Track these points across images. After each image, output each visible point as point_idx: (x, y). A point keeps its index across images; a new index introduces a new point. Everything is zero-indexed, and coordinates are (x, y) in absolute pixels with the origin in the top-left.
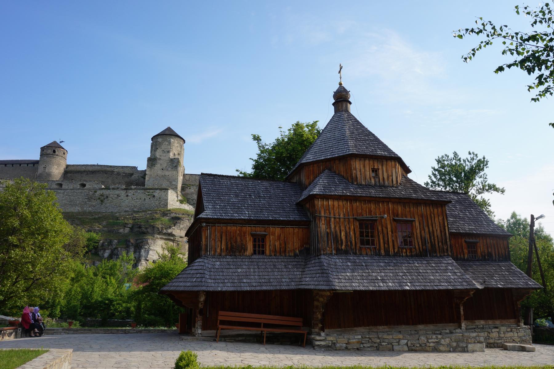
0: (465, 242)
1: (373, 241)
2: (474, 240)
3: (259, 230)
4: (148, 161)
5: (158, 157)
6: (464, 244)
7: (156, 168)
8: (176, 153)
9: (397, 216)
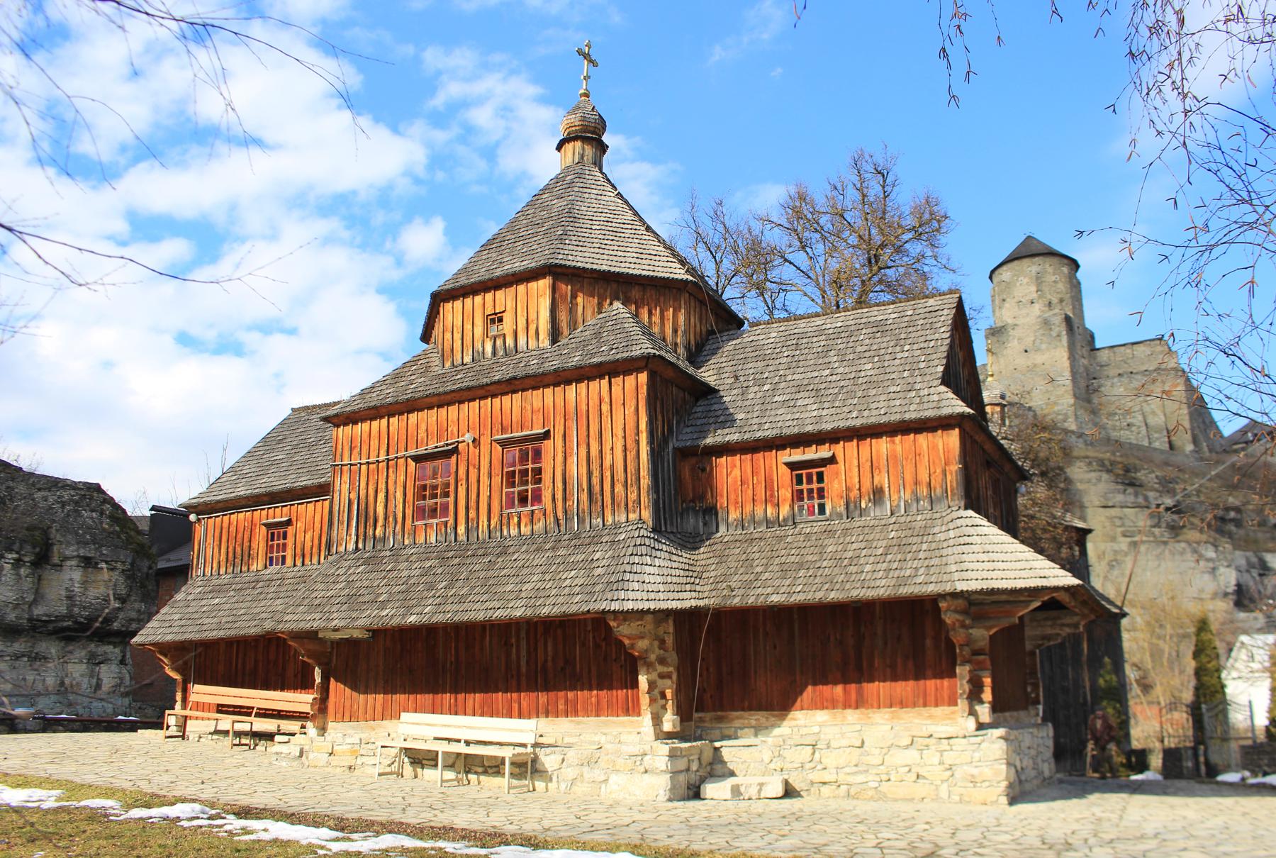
1: (445, 507)
3: (278, 514)
4: (987, 338)
5: (1010, 321)
7: (1008, 352)
8: (1055, 301)
9: (503, 430)
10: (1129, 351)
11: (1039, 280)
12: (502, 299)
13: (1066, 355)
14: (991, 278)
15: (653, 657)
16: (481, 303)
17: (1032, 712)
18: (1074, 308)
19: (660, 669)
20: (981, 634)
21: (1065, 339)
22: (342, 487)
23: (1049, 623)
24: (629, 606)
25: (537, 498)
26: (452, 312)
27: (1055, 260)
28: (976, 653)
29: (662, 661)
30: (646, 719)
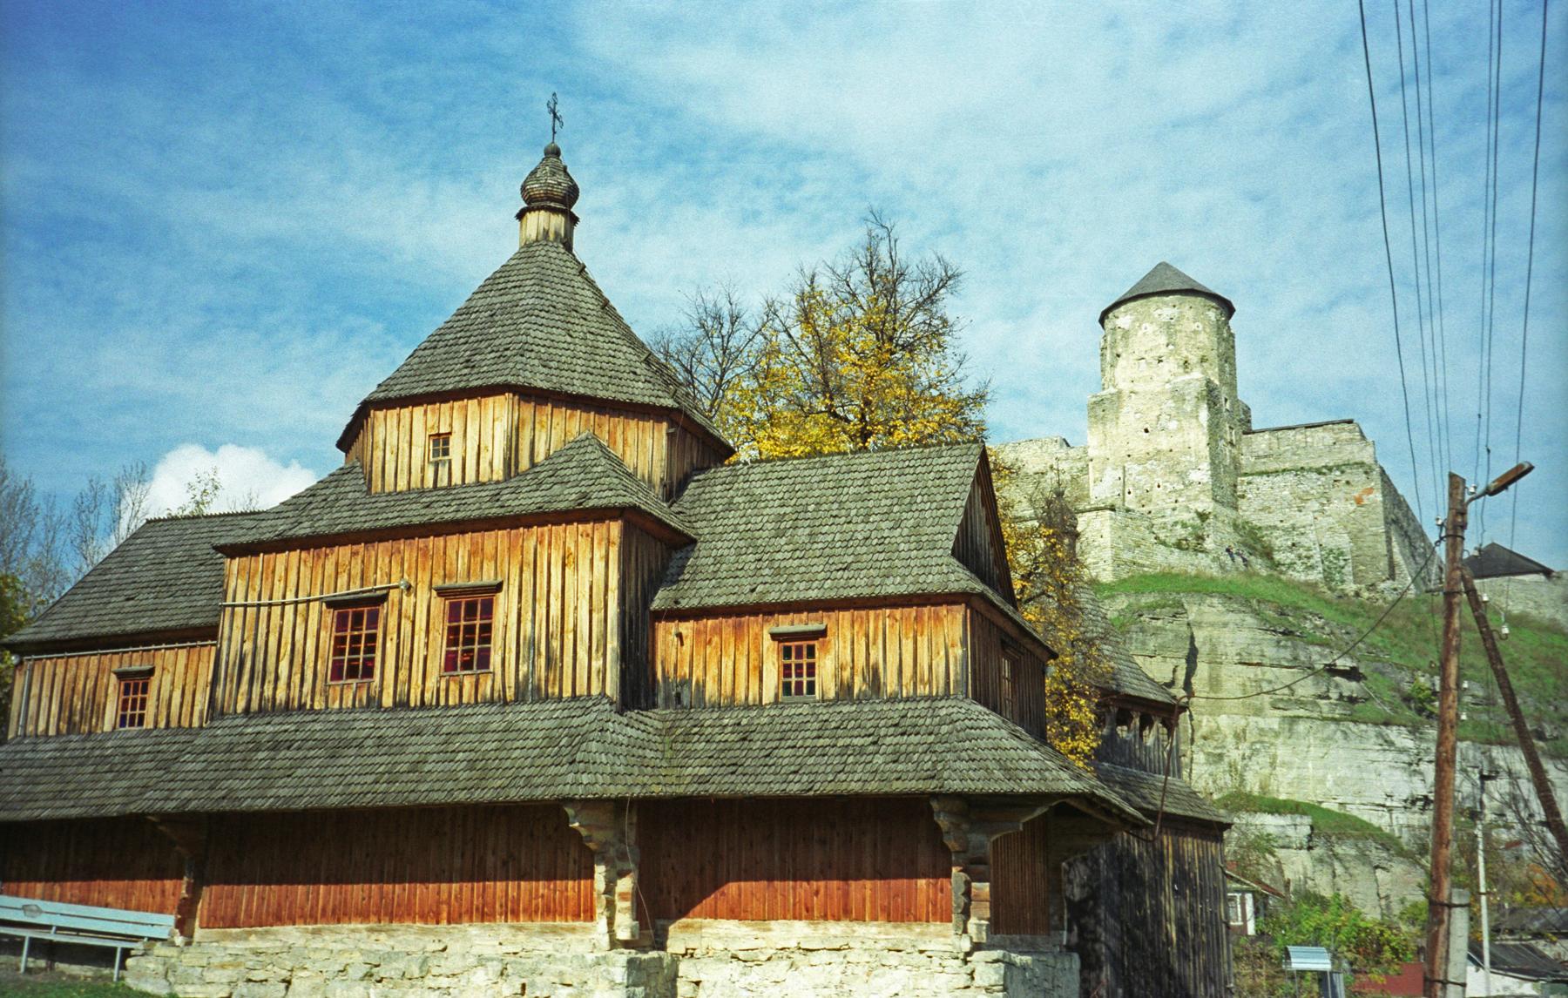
0: (774, 636)
2: (814, 626)
5: (1125, 386)
6: (768, 642)
8: (1194, 359)
10: (1299, 437)
11: (1169, 327)
12: (445, 417)
13: (1205, 439)
14: (1102, 321)
15: (612, 852)
16: (421, 420)
18: (1222, 370)
21: (1204, 414)
22: (233, 635)
25: (484, 661)
26: (385, 426)
27: (1199, 300)
30: (601, 923)
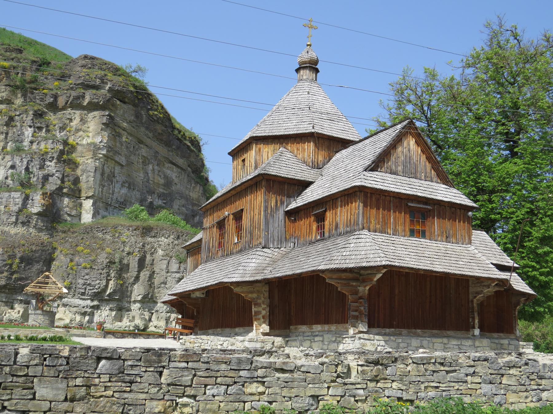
17: (471, 333)
19: (263, 306)
20: (364, 290)
23: (479, 285)
24: (234, 280)
28: (361, 298)
29: (263, 303)
